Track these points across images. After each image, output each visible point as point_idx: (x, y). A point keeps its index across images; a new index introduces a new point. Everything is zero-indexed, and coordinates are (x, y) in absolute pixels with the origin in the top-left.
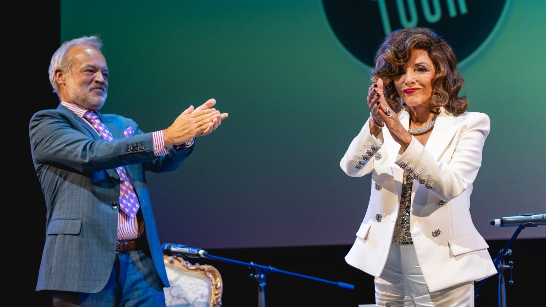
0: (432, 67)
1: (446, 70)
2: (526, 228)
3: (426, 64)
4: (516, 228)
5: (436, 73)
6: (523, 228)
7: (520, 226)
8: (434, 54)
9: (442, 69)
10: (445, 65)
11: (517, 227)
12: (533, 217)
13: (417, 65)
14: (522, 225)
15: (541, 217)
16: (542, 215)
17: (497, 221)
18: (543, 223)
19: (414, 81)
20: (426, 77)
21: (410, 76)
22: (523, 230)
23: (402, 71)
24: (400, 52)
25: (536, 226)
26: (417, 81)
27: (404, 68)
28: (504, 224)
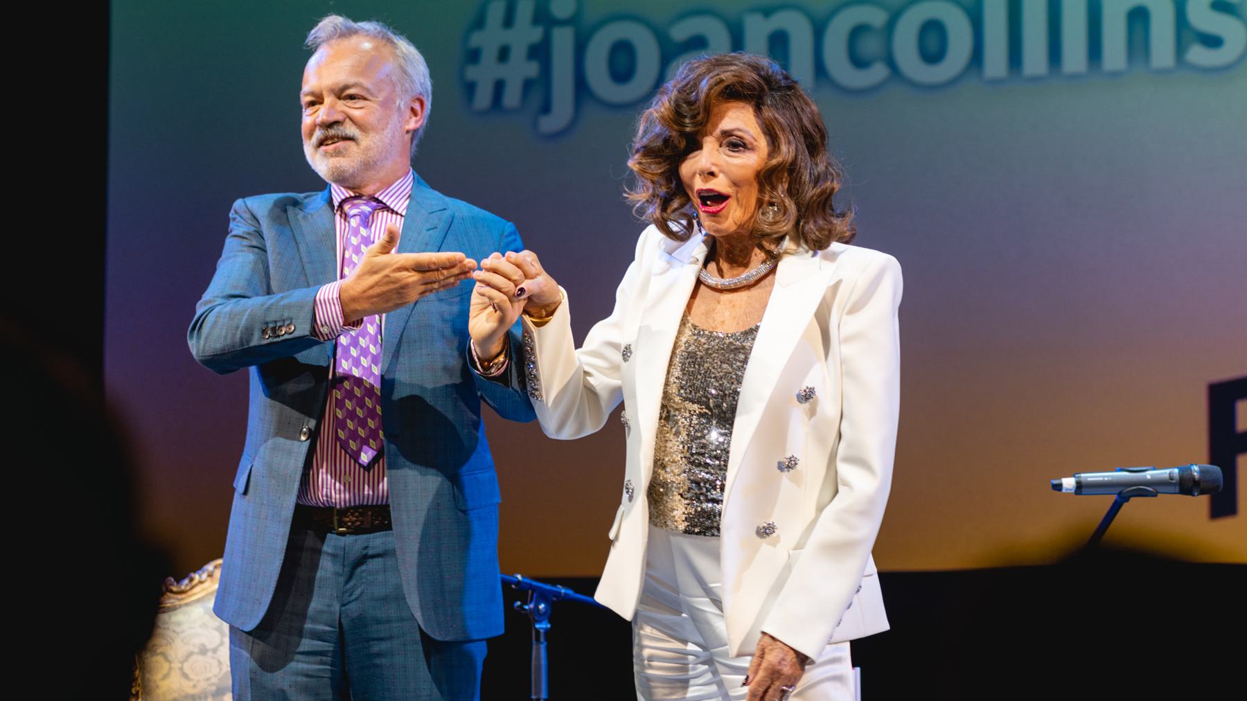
0: (763, 143)
1: (793, 148)
2: (1132, 499)
3: (746, 132)
4: (1110, 499)
5: (771, 155)
6: (1127, 499)
7: (1119, 494)
8: (768, 113)
9: (784, 148)
10: (791, 138)
11: (1114, 497)
12: (1149, 475)
13: (727, 134)
14: (1124, 493)
15: (1167, 476)
16: (1168, 471)
17: (1069, 483)
18: (1171, 489)
19: (714, 169)
20: (749, 162)
21: (709, 155)
22: (1125, 505)
23: (694, 145)
24: (690, 103)
25: (1154, 495)
26: (722, 171)
27: (699, 137)
28: (1084, 491)
